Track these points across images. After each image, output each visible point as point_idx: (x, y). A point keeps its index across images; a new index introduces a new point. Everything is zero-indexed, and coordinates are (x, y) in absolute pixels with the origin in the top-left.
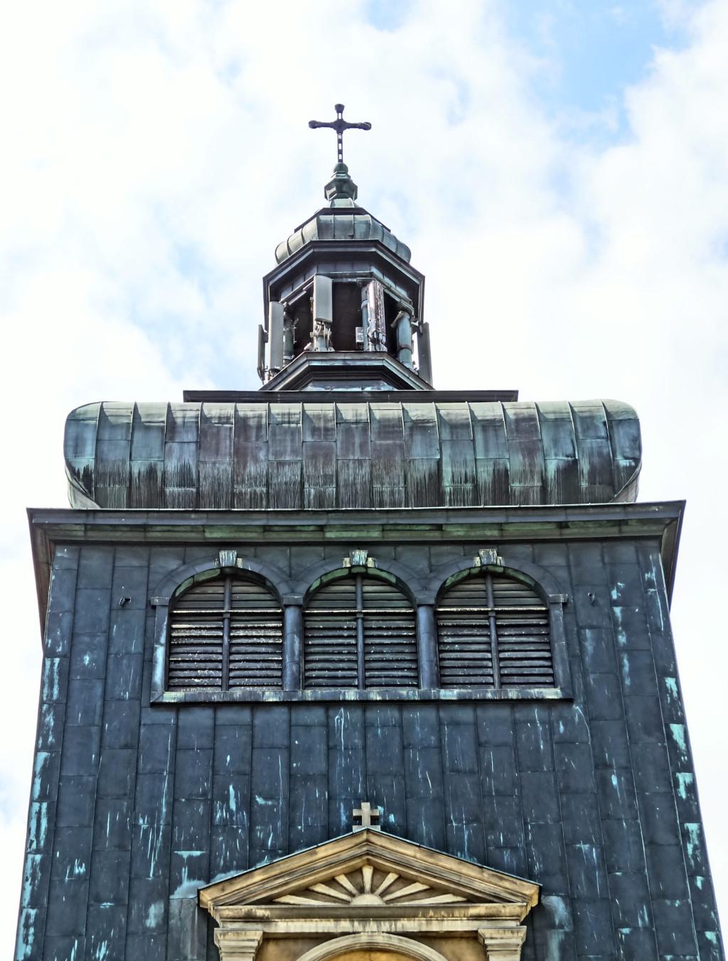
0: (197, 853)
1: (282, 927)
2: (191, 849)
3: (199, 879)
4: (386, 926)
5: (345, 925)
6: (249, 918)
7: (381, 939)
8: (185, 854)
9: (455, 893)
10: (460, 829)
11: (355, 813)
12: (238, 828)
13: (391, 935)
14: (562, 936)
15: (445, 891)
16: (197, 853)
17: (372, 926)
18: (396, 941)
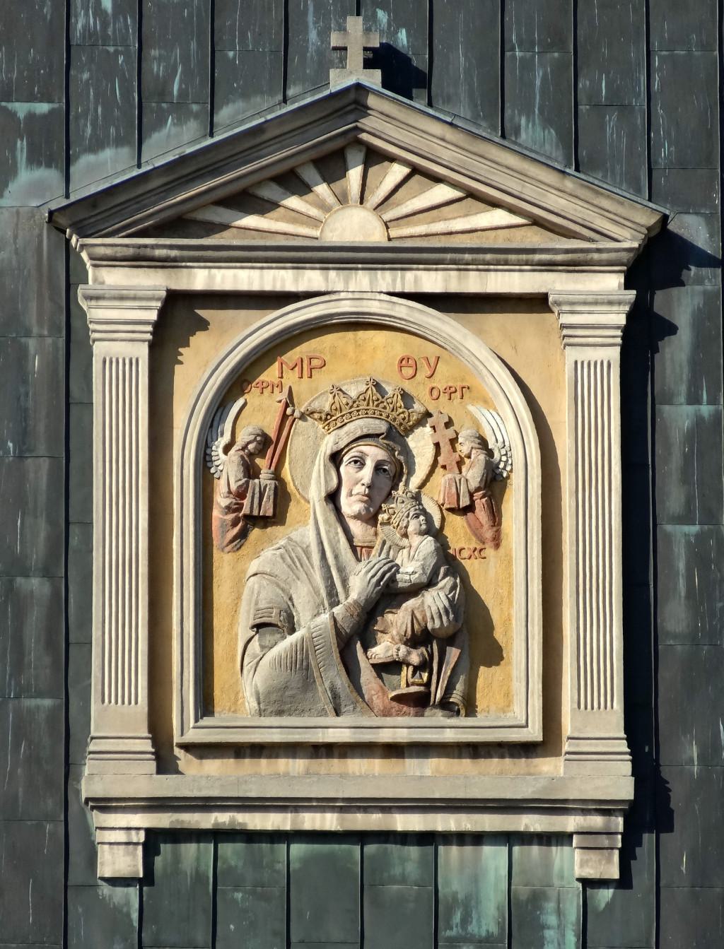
0: (43, 108)
1: (200, 279)
2: (31, 98)
3: (49, 166)
4: (386, 280)
5: (311, 279)
6: (139, 260)
7: (376, 307)
8: (21, 109)
9: (512, 210)
10: (527, 65)
11: (335, 40)
12: (117, 53)
13: (395, 299)
14: (698, 301)
15: (495, 204)
16: (43, 108)
17: (361, 280)
18: (406, 311)
